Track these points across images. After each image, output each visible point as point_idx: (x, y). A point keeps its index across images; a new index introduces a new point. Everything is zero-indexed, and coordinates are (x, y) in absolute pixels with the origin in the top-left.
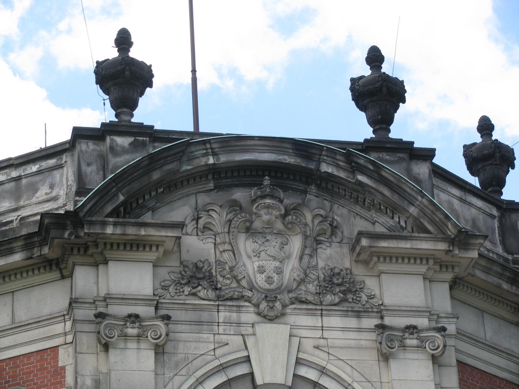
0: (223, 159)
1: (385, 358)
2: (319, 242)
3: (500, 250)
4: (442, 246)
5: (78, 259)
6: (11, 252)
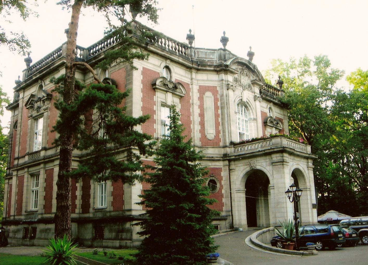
5: (223, 72)
6: (211, 67)
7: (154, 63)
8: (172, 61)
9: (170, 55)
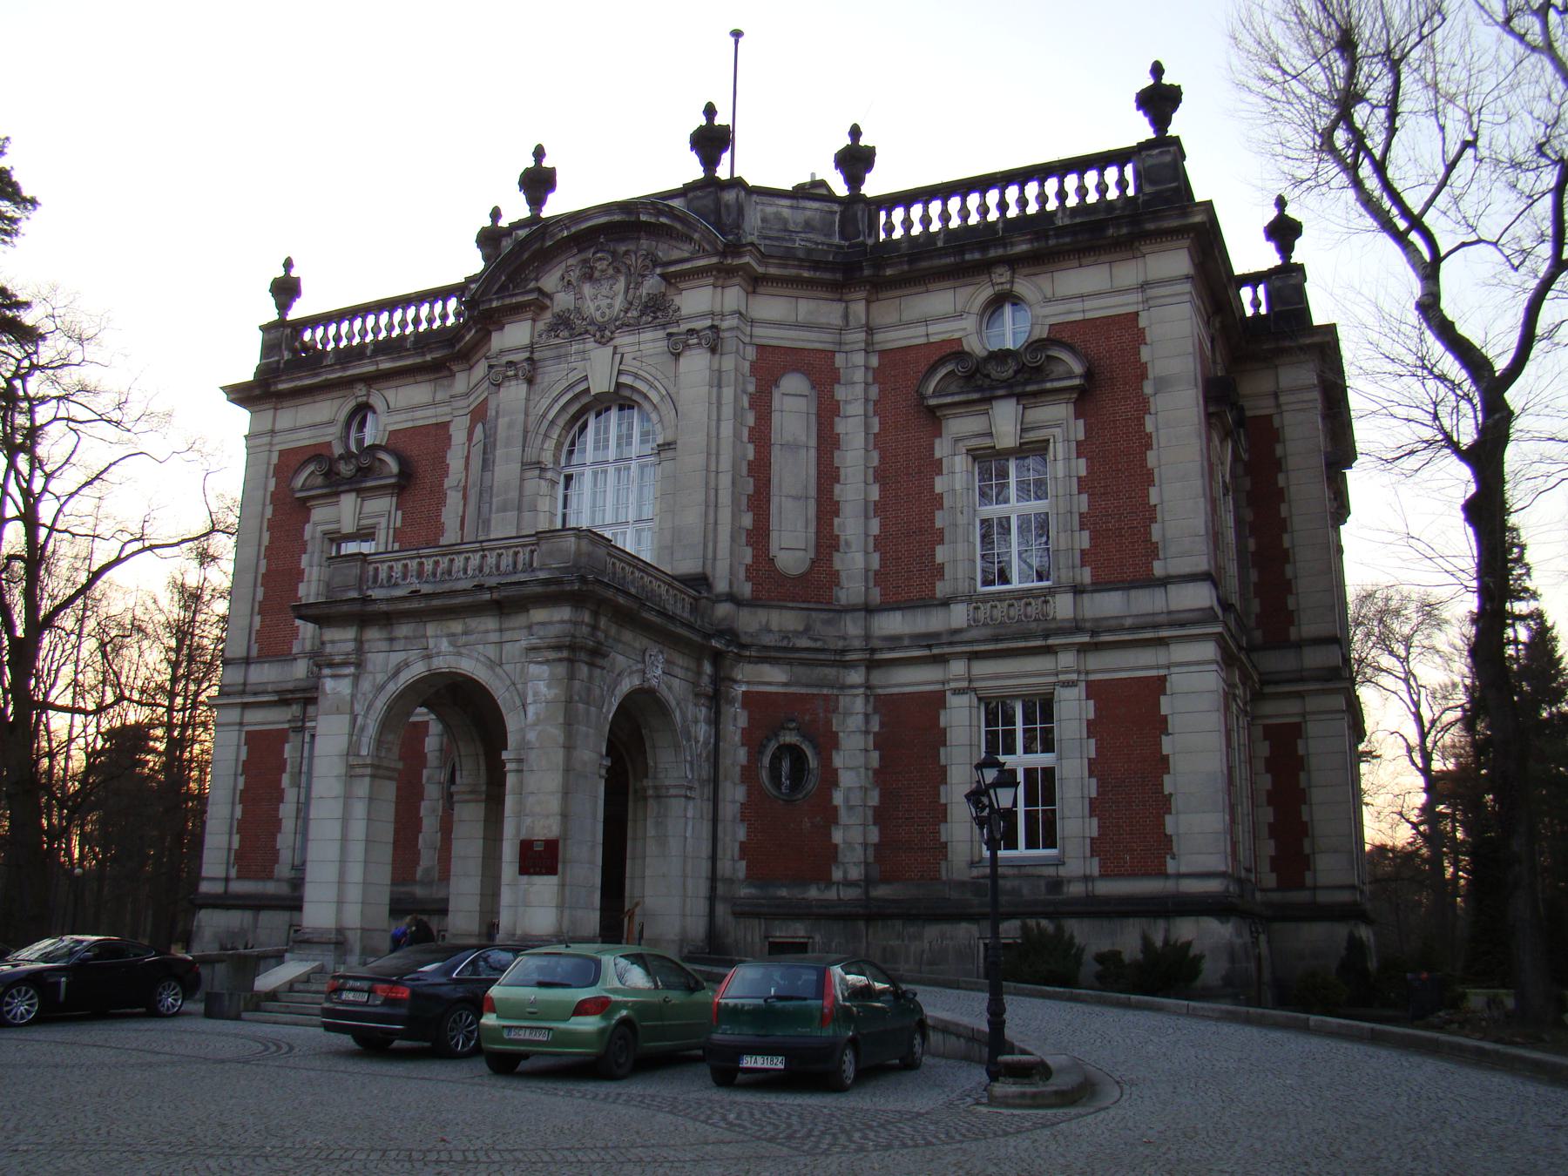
0: (573, 230)
1: (677, 356)
2: (644, 276)
3: (836, 240)
4: (714, 260)
7: (318, 419)
8: (370, 380)
9: (344, 369)
